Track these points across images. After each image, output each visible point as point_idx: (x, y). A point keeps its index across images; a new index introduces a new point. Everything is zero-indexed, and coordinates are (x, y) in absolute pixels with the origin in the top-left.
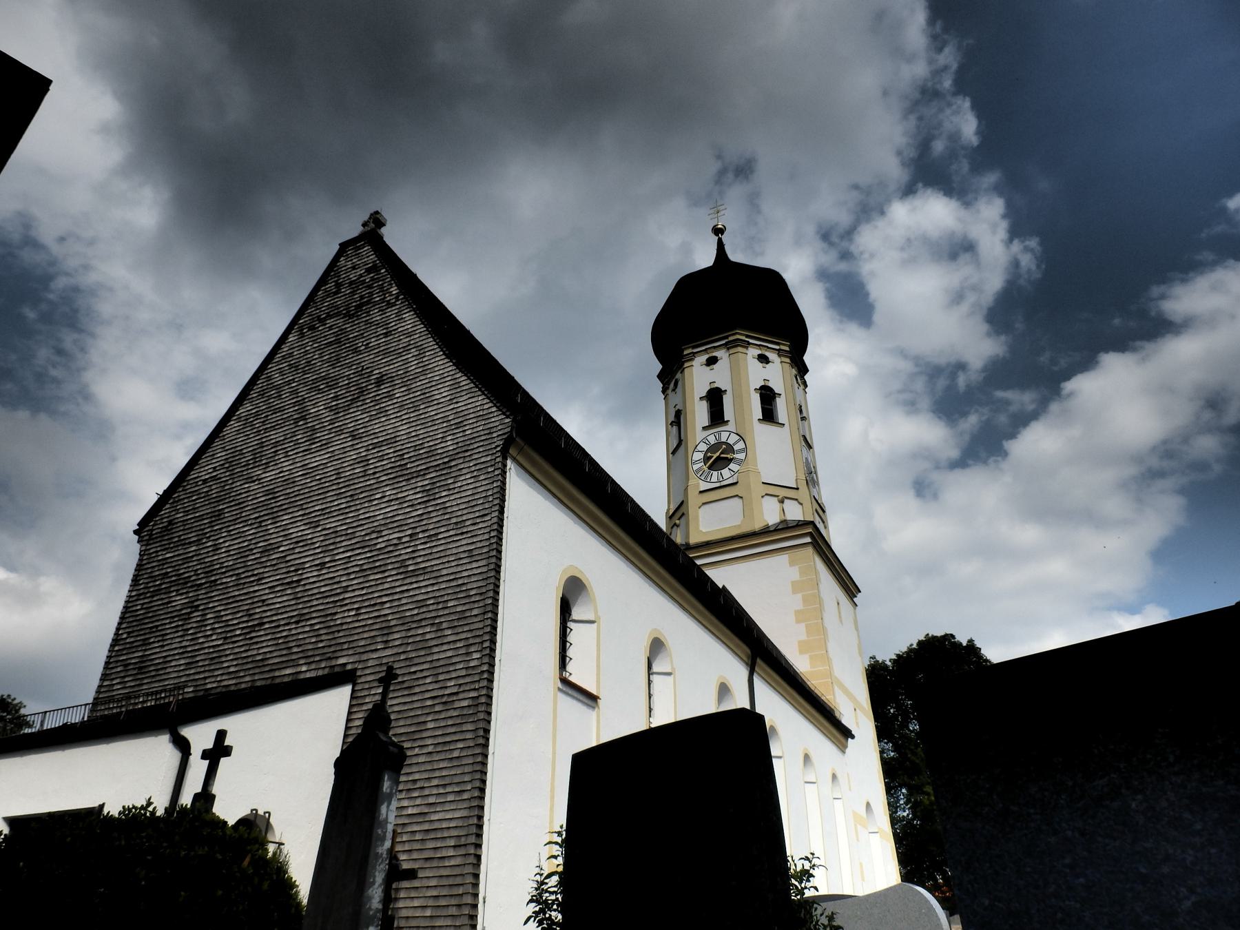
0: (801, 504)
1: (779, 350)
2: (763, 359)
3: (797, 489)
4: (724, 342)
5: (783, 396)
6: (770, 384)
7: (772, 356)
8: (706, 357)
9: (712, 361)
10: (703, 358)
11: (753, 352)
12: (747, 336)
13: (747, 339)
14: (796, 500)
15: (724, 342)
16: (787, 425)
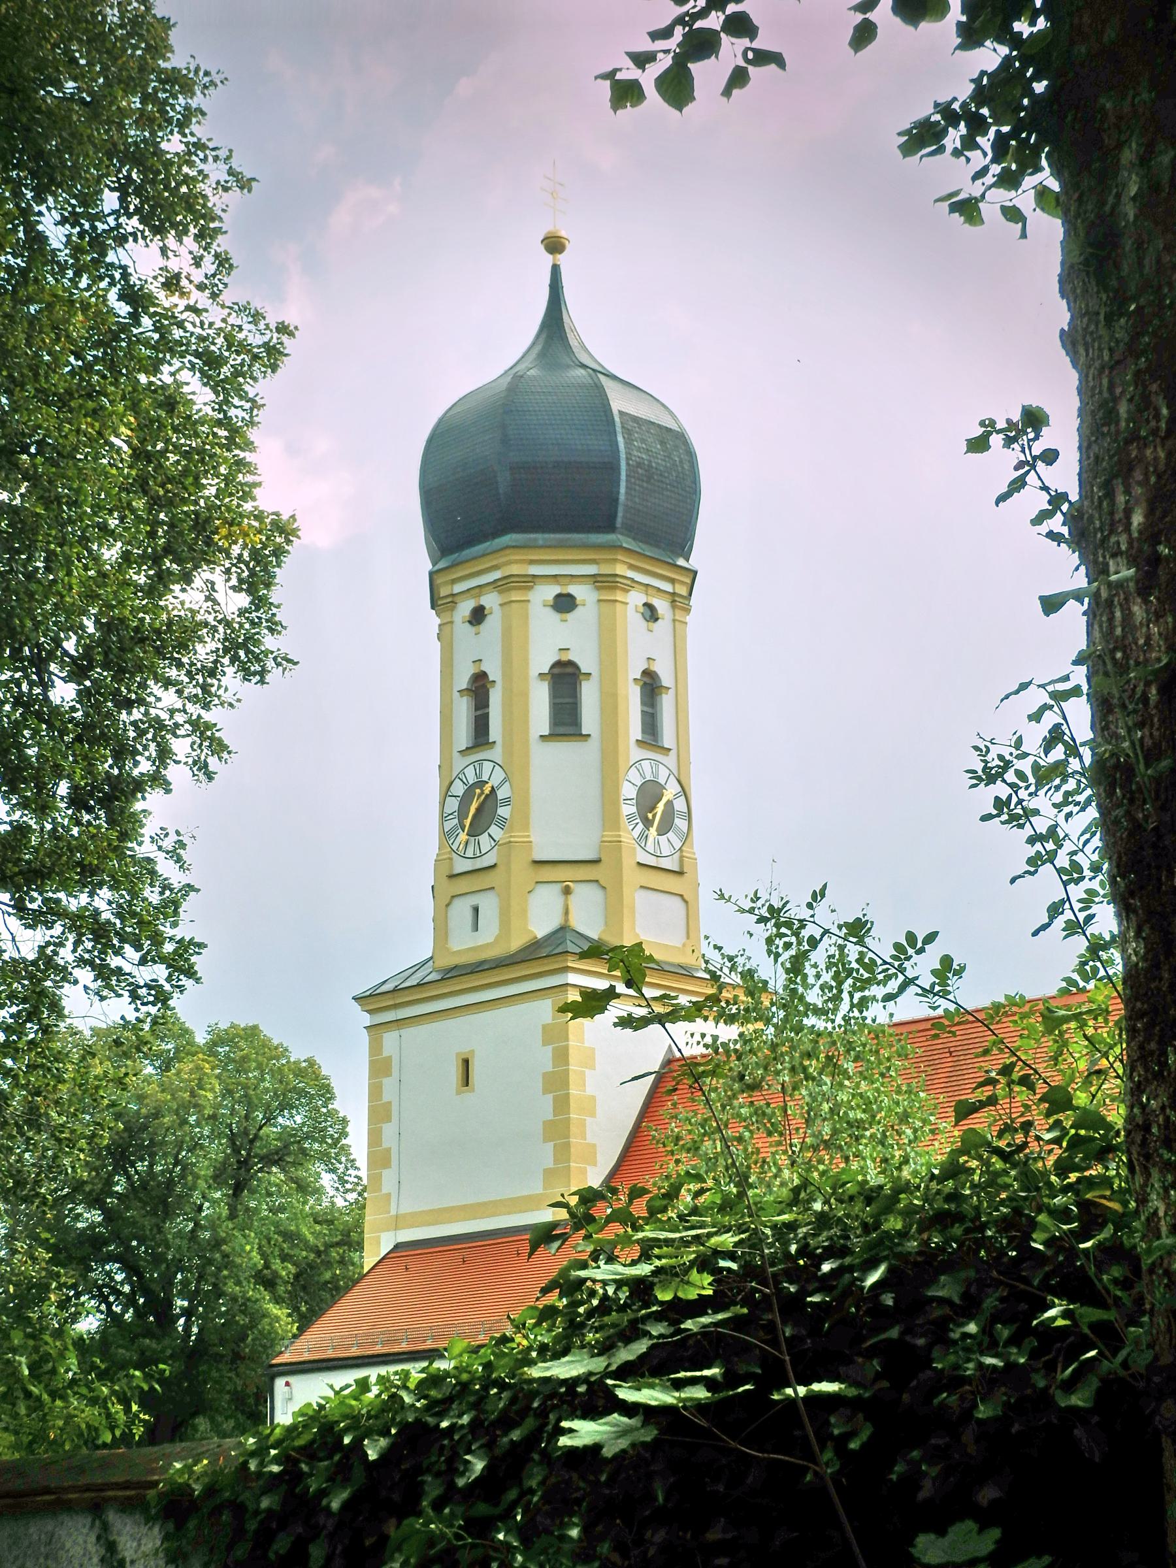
0: (686, 902)
1: (674, 594)
2: (651, 613)
3: (680, 873)
4: (591, 570)
5: (671, 692)
6: (655, 667)
7: (662, 605)
8: (556, 590)
9: (564, 604)
10: (550, 592)
11: (636, 599)
12: (632, 567)
13: (630, 574)
14: (681, 896)
15: (591, 570)
16: (673, 754)
